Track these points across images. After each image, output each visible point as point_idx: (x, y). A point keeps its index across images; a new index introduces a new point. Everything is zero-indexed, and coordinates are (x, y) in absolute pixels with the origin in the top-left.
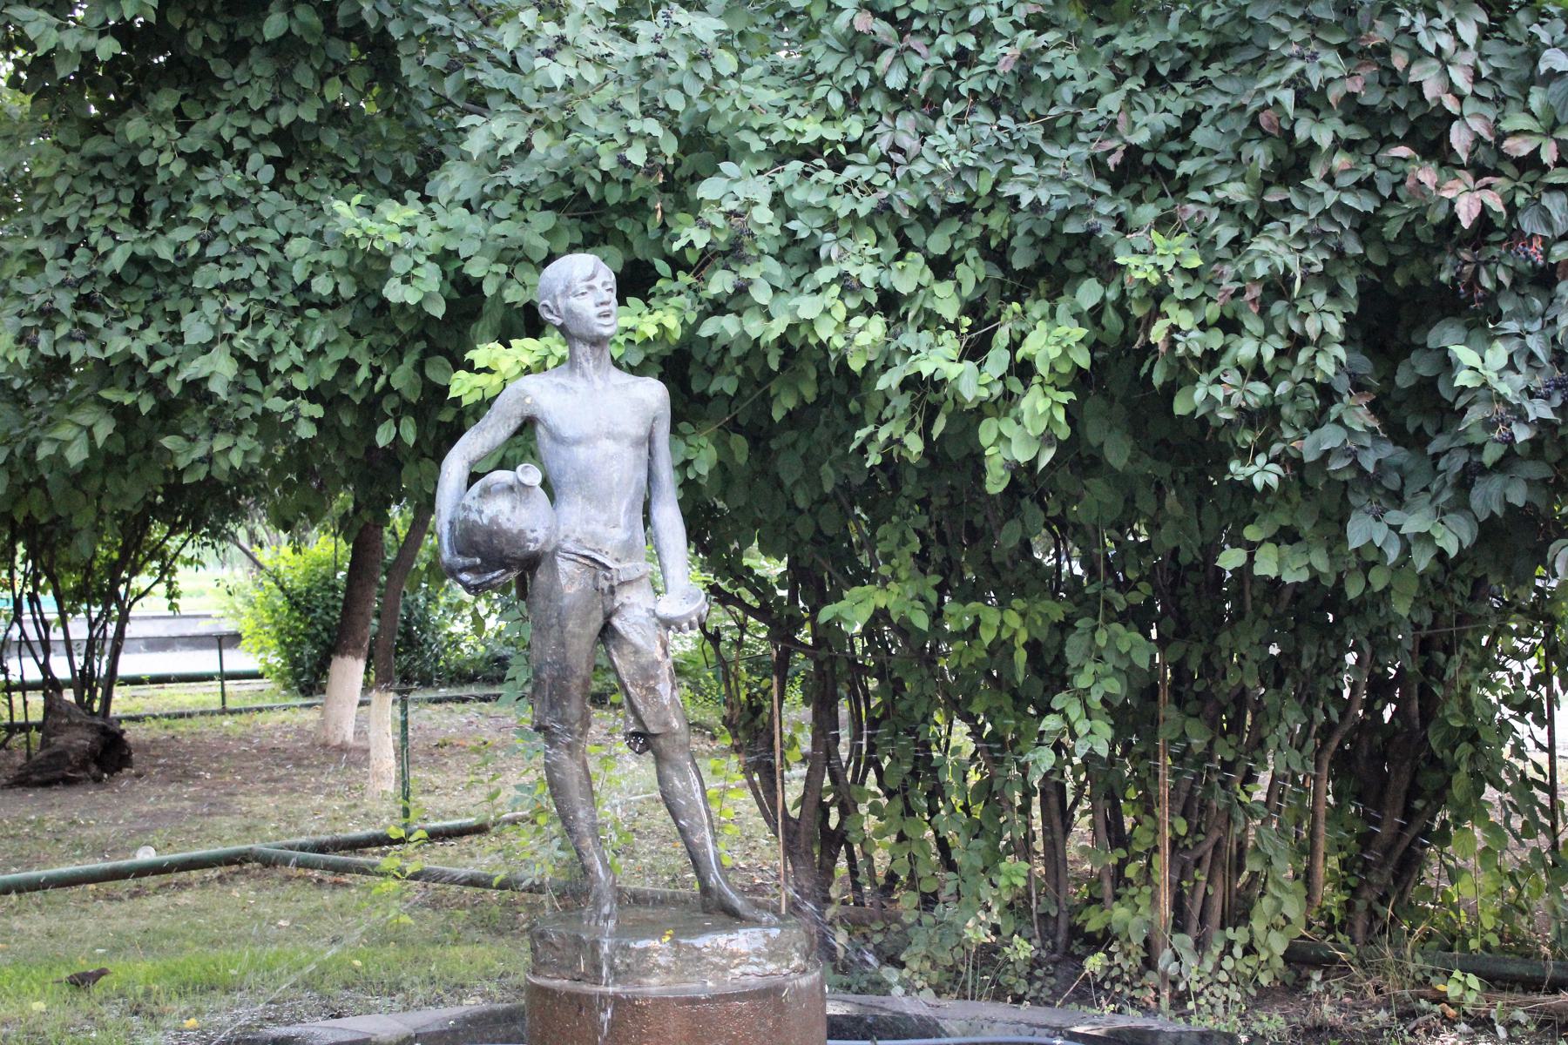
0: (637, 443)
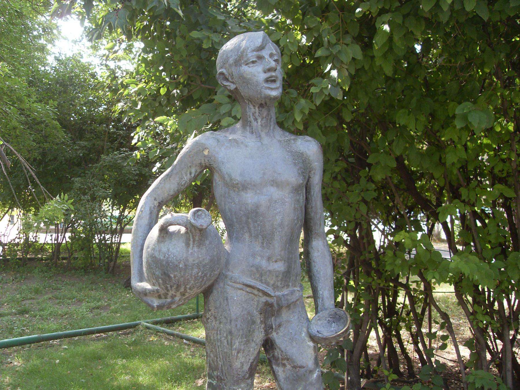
0: (296, 190)
